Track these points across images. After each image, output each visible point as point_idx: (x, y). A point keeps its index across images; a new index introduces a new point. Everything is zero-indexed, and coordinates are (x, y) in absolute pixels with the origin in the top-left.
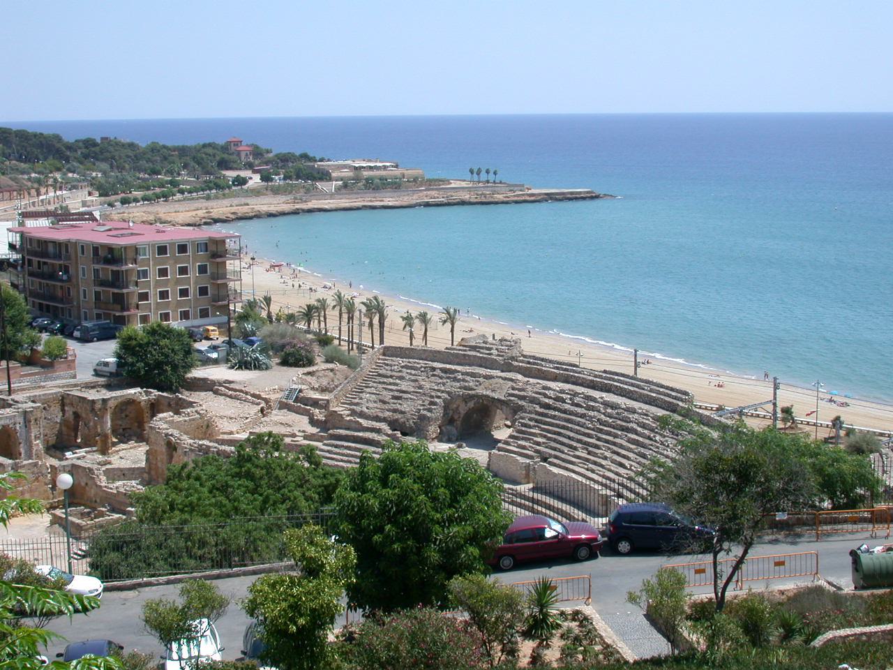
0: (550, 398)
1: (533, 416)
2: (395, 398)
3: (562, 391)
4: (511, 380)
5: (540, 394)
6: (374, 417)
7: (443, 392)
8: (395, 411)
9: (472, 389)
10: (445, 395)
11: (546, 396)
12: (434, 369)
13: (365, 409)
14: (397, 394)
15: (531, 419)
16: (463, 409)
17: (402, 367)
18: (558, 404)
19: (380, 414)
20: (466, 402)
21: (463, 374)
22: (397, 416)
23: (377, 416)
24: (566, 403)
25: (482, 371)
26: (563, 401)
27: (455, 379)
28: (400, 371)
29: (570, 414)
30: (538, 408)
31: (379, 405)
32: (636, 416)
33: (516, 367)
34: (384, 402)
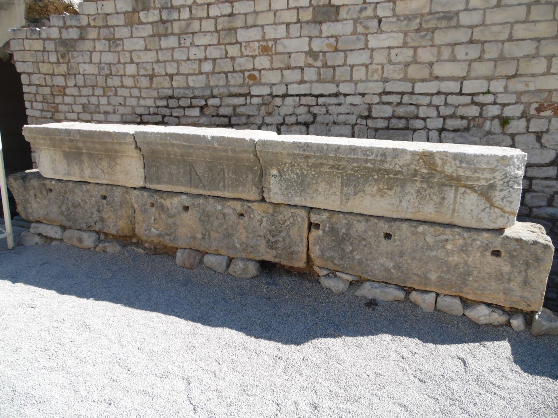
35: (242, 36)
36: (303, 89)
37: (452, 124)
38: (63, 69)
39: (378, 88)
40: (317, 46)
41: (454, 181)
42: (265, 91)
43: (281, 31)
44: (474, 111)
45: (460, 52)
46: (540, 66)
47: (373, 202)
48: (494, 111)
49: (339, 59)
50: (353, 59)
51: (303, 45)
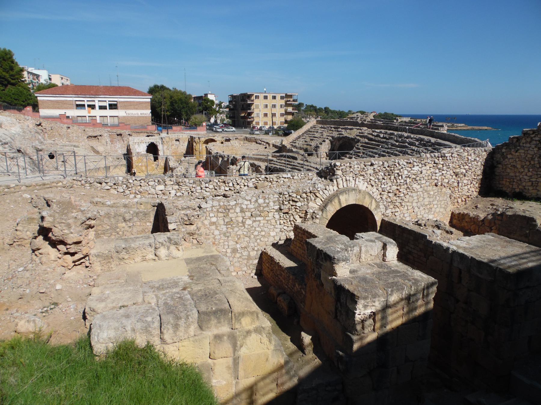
0: (374, 135)
2: (311, 140)
3: (381, 132)
4: (361, 129)
8: (307, 145)
9: (342, 134)
10: (331, 138)
12: (331, 128)
13: (297, 145)
14: (312, 138)
15: (361, 146)
16: (338, 144)
18: (377, 139)
19: (302, 147)
22: (308, 147)
24: (380, 137)
25: (349, 127)
27: (338, 131)
30: (367, 141)
31: (304, 143)
32: (410, 140)
34: (306, 141)
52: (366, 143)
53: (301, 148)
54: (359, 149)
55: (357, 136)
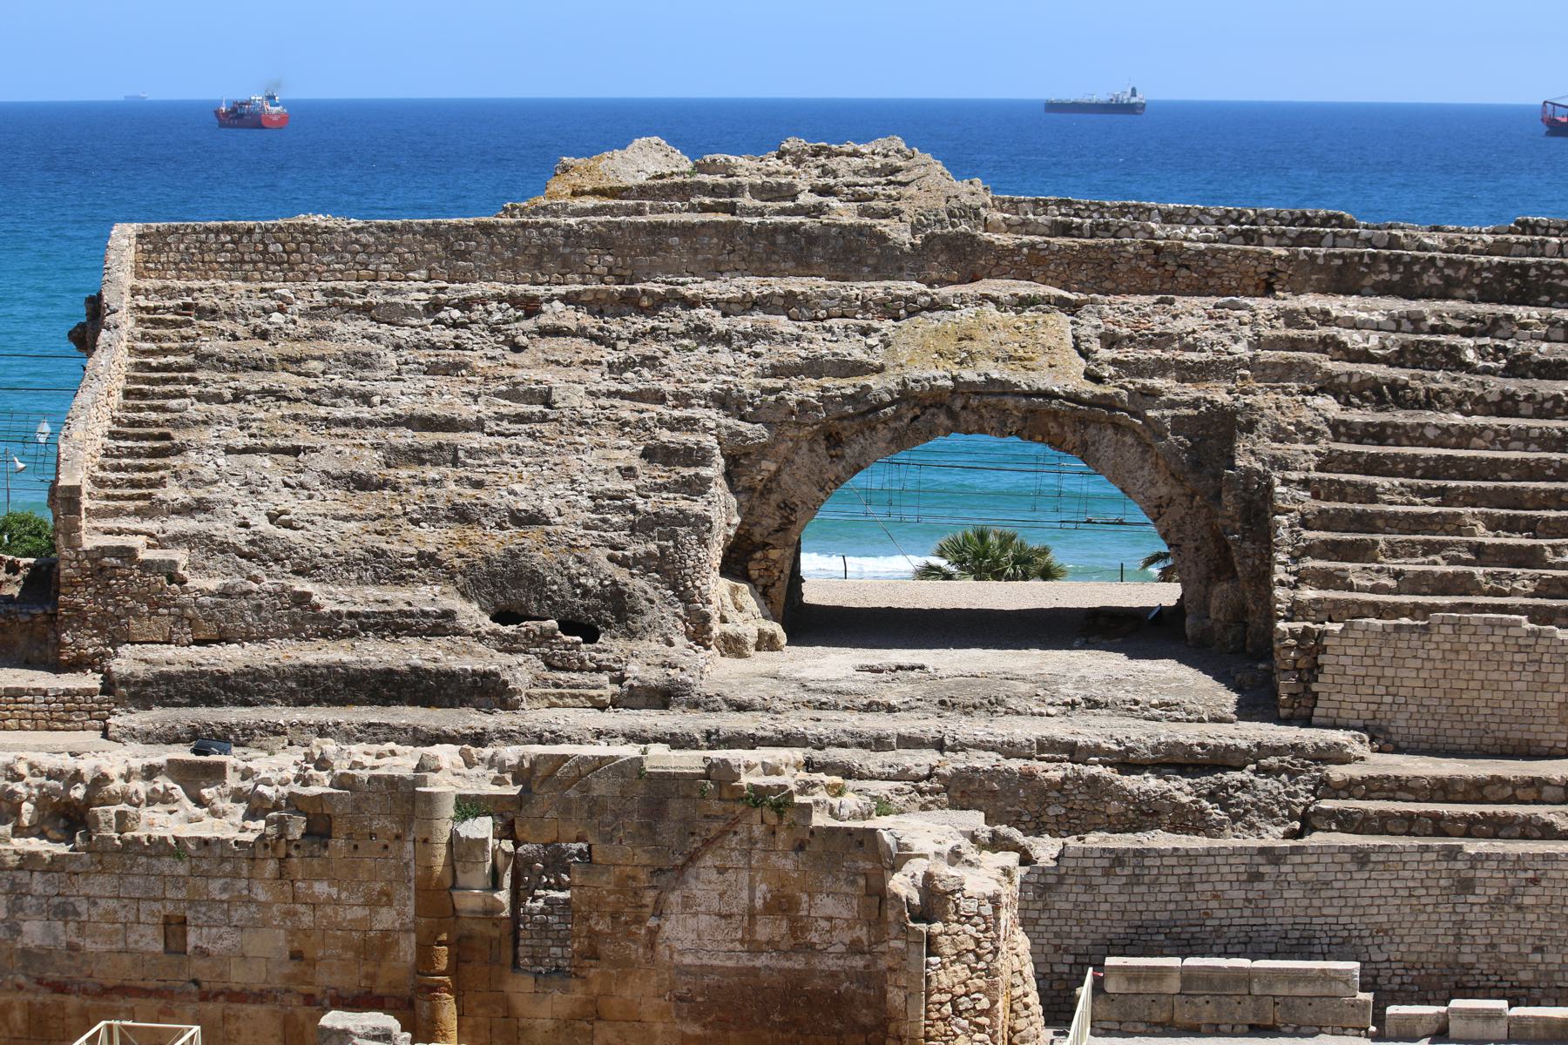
0: (1365, 356)
1: (1323, 445)
2: (416, 456)
5: (1294, 344)
6: (349, 564)
7: (683, 400)
8: (461, 515)
9: (859, 369)
11: (1329, 345)
12: (531, 307)
17: (313, 313)
20: (833, 440)
21: (727, 307)
23: (379, 554)
26: (1453, 359)
27: (701, 333)
28: (320, 335)
29: (1538, 414)
30: (1329, 405)
31: (337, 500)
33: (1003, 253)
34: (362, 483)
35: (1198, 887)
36: (1243, 921)
37: (1334, 941)
38: (1040, 905)
39: (1291, 920)
40: (1251, 895)
41: (1334, 979)
42: (1216, 922)
43: (1227, 886)
44: (1345, 933)
45: (1335, 902)
46: (1375, 910)
47: (1302, 990)
48: (1356, 933)
49: (1265, 903)
50: (1274, 904)
51: (1242, 894)
52: (1340, 429)
53: (381, 566)
54: (1371, 495)
55: (1137, 368)
